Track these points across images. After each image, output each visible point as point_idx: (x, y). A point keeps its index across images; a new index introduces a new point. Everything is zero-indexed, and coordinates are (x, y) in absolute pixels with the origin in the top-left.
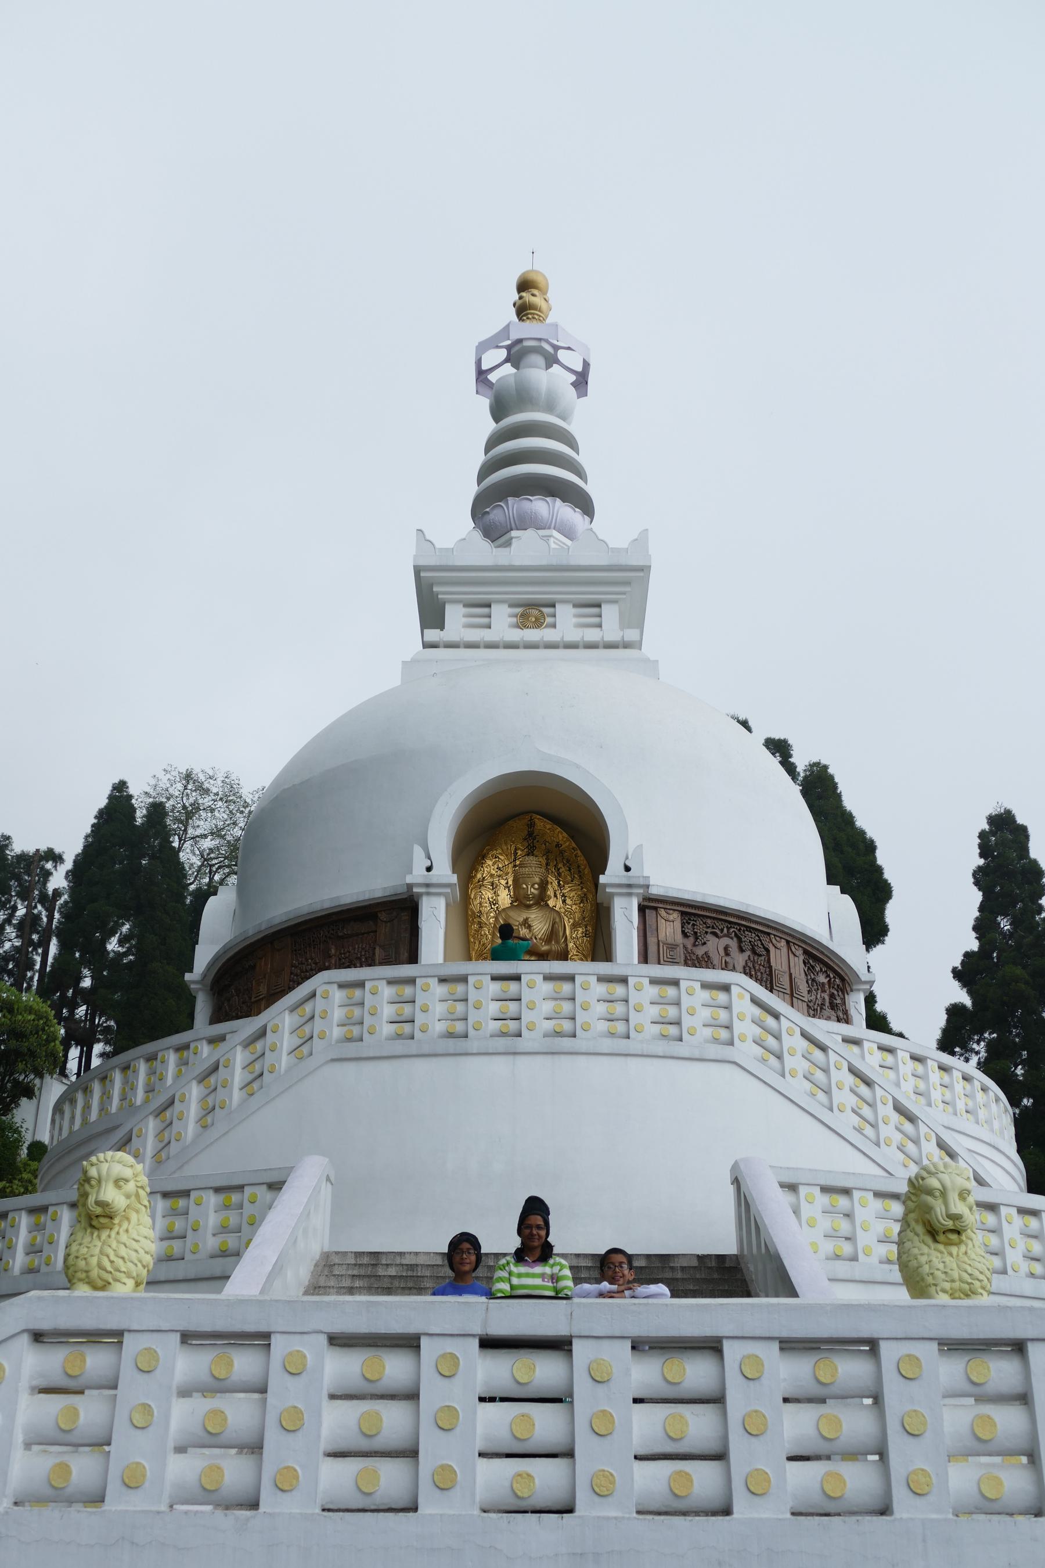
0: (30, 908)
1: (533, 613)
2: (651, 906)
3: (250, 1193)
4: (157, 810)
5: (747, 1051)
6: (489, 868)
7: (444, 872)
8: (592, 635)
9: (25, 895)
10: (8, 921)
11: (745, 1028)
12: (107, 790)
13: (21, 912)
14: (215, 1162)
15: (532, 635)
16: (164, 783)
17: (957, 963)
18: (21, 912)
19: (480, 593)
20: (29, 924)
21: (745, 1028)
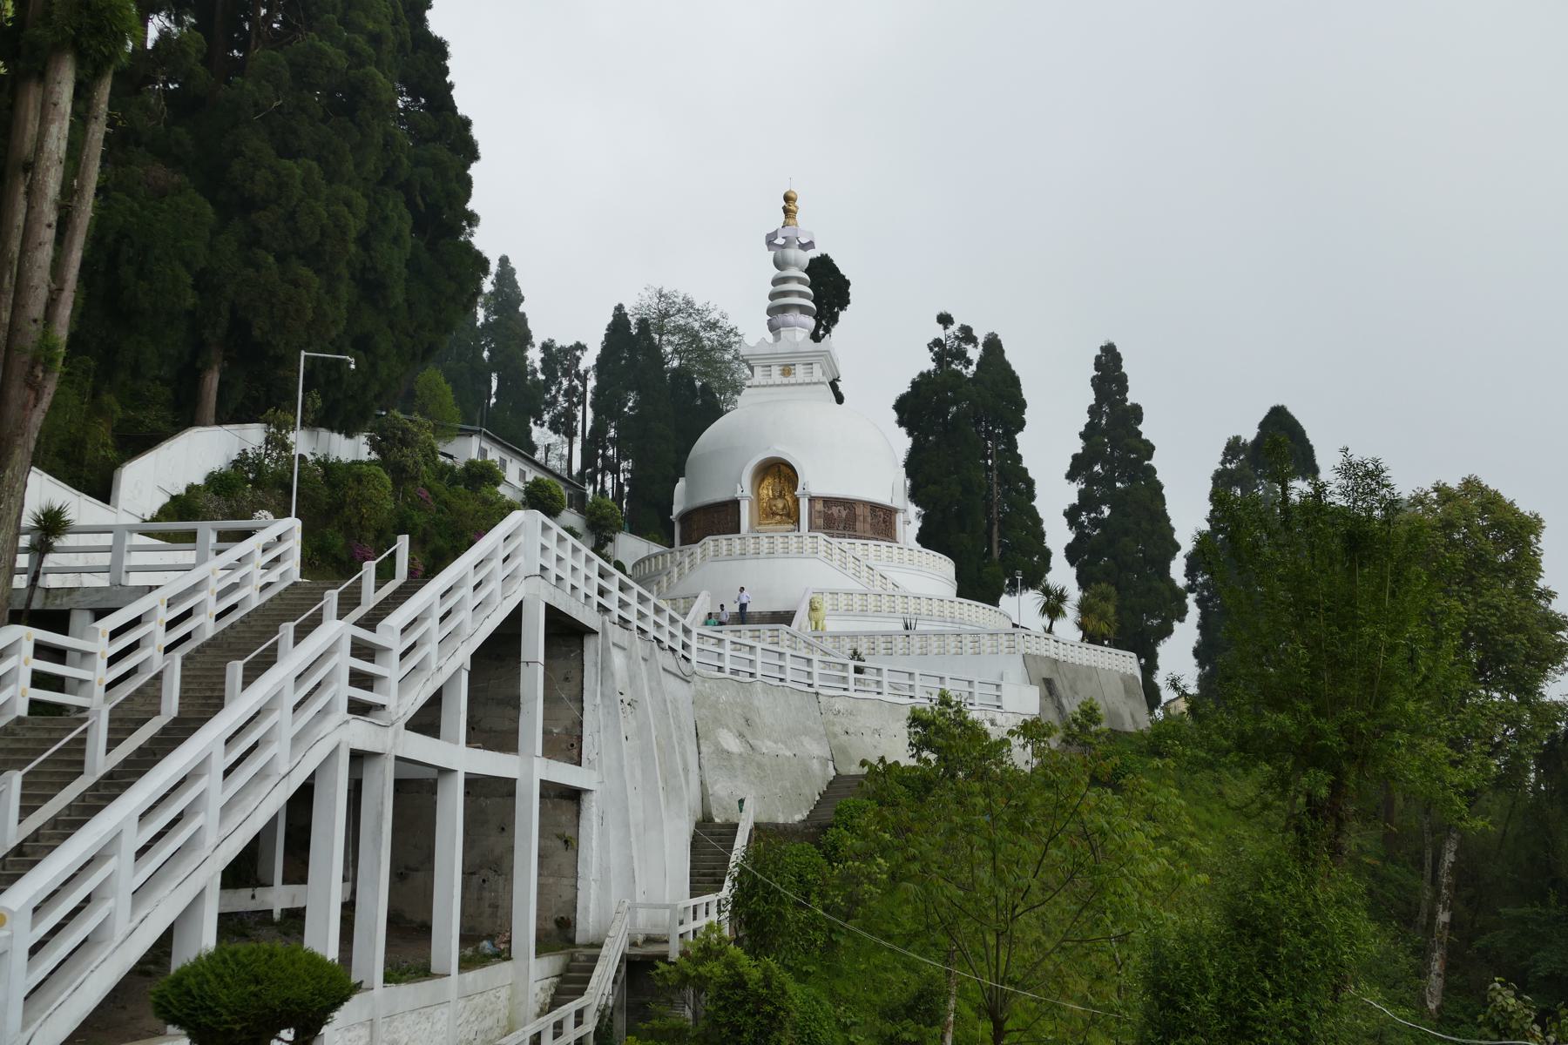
0: (571, 381)
1: (787, 370)
2: (812, 500)
3: (690, 599)
4: (643, 323)
5: (822, 554)
6: (768, 481)
7: (747, 492)
8: (807, 380)
9: (566, 373)
10: (558, 391)
11: (822, 548)
12: (611, 311)
13: (565, 383)
14: (680, 590)
15: (785, 380)
16: (648, 301)
17: (1082, 429)
18: (565, 383)
19: (767, 362)
20: (571, 391)
21: (822, 548)
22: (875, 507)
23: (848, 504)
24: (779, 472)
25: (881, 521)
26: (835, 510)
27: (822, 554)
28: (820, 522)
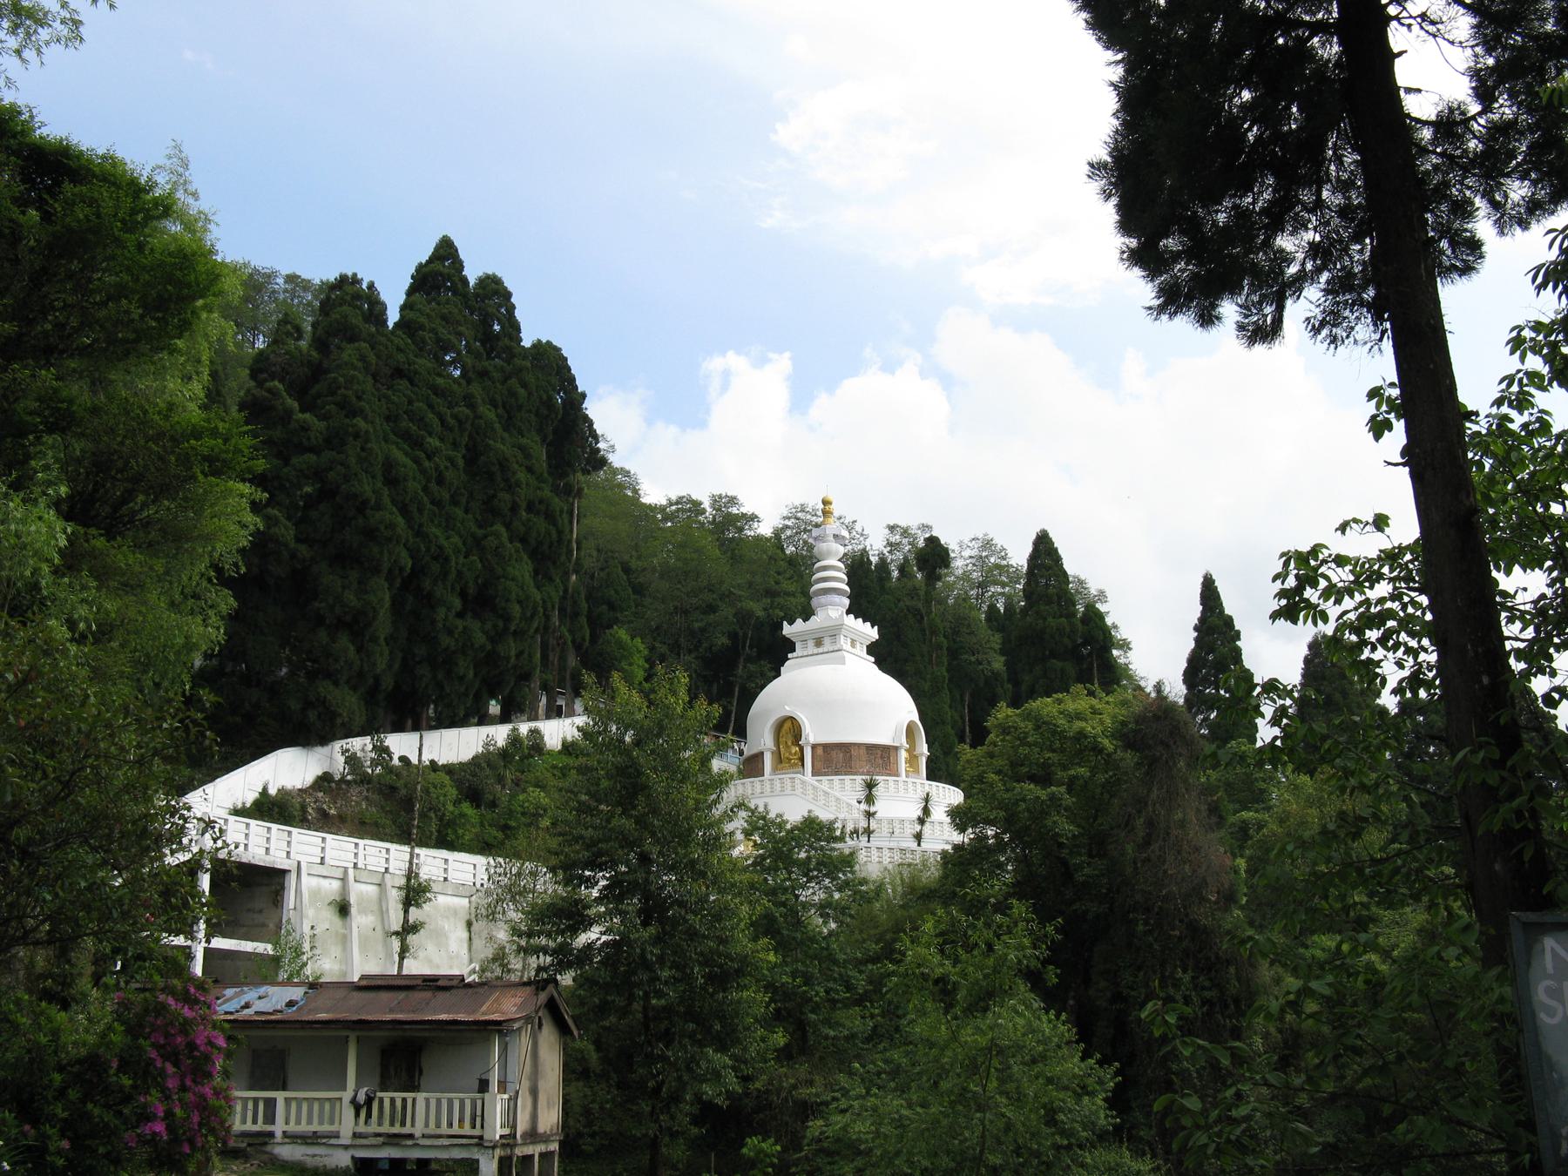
2: (814, 747)
22: (871, 748)
23: (845, 748)
24: (789, 729)
25: (879, 757)
26: (834, 754)
27: (799, 791)
28: (818, 764)
